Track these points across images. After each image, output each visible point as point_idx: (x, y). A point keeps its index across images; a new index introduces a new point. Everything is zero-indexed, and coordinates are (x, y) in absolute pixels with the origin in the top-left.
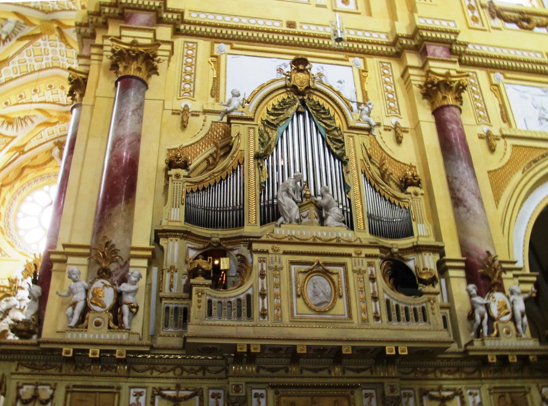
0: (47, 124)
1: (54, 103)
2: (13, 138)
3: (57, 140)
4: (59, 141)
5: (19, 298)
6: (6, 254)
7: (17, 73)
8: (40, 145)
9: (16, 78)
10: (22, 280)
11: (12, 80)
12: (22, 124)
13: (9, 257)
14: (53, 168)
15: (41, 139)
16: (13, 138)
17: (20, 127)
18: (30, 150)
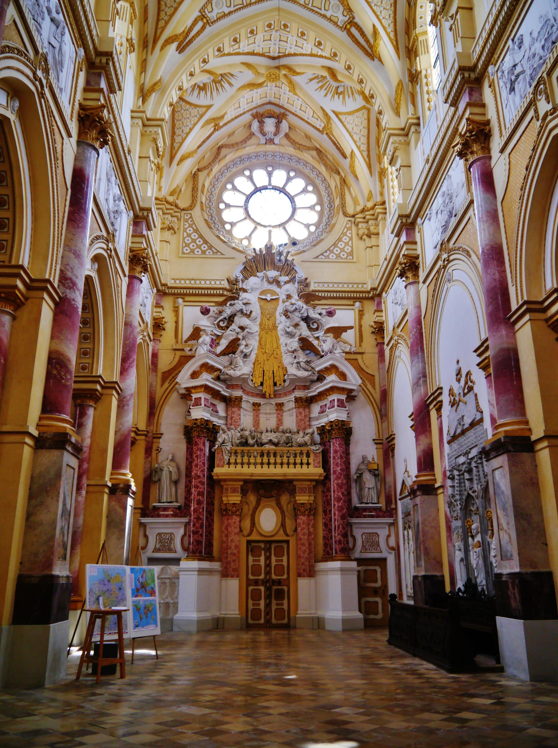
0: (252, 86)
1: (262, 55)
2: (209, 107)
3: (254, 111)
4: (257, 113)
5: (245, 301)
6: (218, 251)
7: (230, 6)
8: (236, 117)
9: (230, 13)
10: (243, 281)
11: (225, 15)
12: (217, 89)
13: (222, 254)
14: (254, 147)
15: (239, 109)
16: (209, 107)
17: (215, 93)
18: (225, 124)
